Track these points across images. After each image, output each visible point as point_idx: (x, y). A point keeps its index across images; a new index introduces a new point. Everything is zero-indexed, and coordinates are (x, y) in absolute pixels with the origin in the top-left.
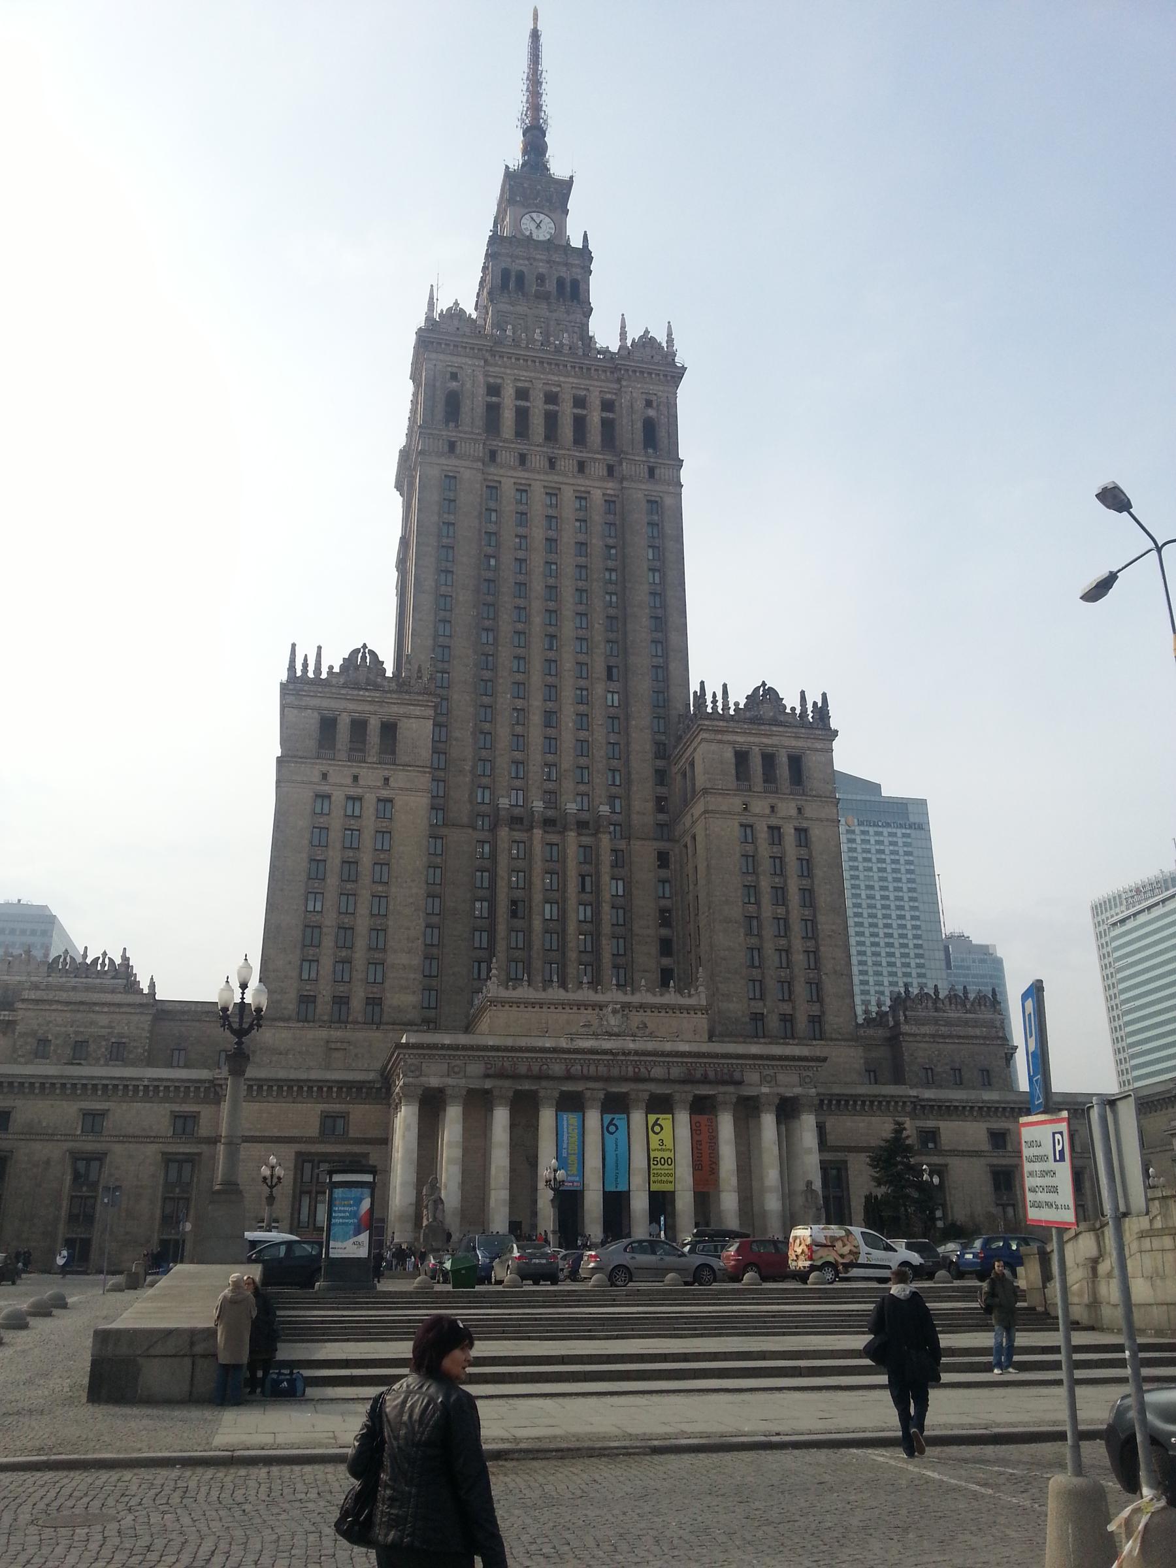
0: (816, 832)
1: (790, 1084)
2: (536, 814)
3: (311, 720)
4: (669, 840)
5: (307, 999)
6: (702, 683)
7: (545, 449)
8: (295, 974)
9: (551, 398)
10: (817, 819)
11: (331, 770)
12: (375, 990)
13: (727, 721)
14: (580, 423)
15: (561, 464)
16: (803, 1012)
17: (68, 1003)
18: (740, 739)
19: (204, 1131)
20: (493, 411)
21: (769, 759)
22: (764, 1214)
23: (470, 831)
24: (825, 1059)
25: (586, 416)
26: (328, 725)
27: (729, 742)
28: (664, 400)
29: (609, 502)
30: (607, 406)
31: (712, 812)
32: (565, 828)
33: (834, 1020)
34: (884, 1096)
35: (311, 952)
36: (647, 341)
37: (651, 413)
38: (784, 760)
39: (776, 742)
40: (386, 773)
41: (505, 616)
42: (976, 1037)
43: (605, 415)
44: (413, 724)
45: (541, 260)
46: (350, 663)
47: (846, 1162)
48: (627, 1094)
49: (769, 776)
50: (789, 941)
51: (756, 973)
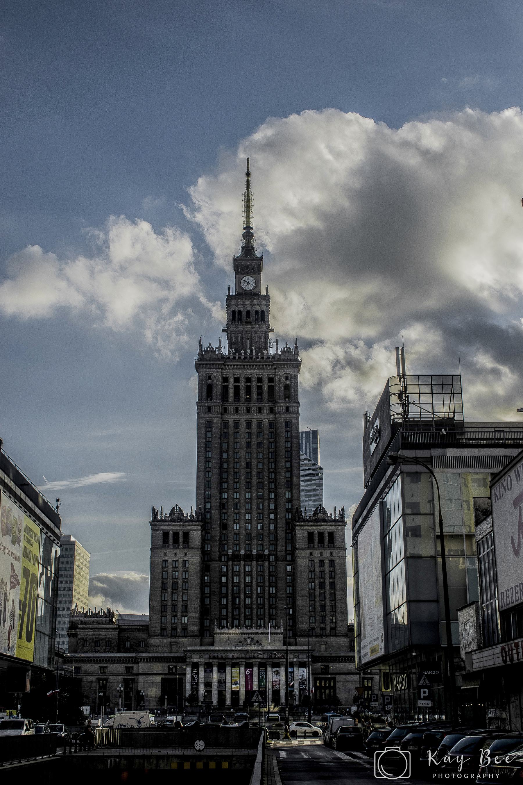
0: (337, 561)
3: (160, 534)
5: (163, 629)
8: (159, 621)
9: (248, 380)
11: (167, 551)
15: (253, 410)
17: (92, 629)
18: (310, 528)
19: (135, 672)
20: (225, 389)
25: (262, 386)
26: (166, 535)
27: (306, 530)
29: (270, 424)
30: (271, 380)
34: (350, 656)
37: (288, 382)
44: (194, 533)
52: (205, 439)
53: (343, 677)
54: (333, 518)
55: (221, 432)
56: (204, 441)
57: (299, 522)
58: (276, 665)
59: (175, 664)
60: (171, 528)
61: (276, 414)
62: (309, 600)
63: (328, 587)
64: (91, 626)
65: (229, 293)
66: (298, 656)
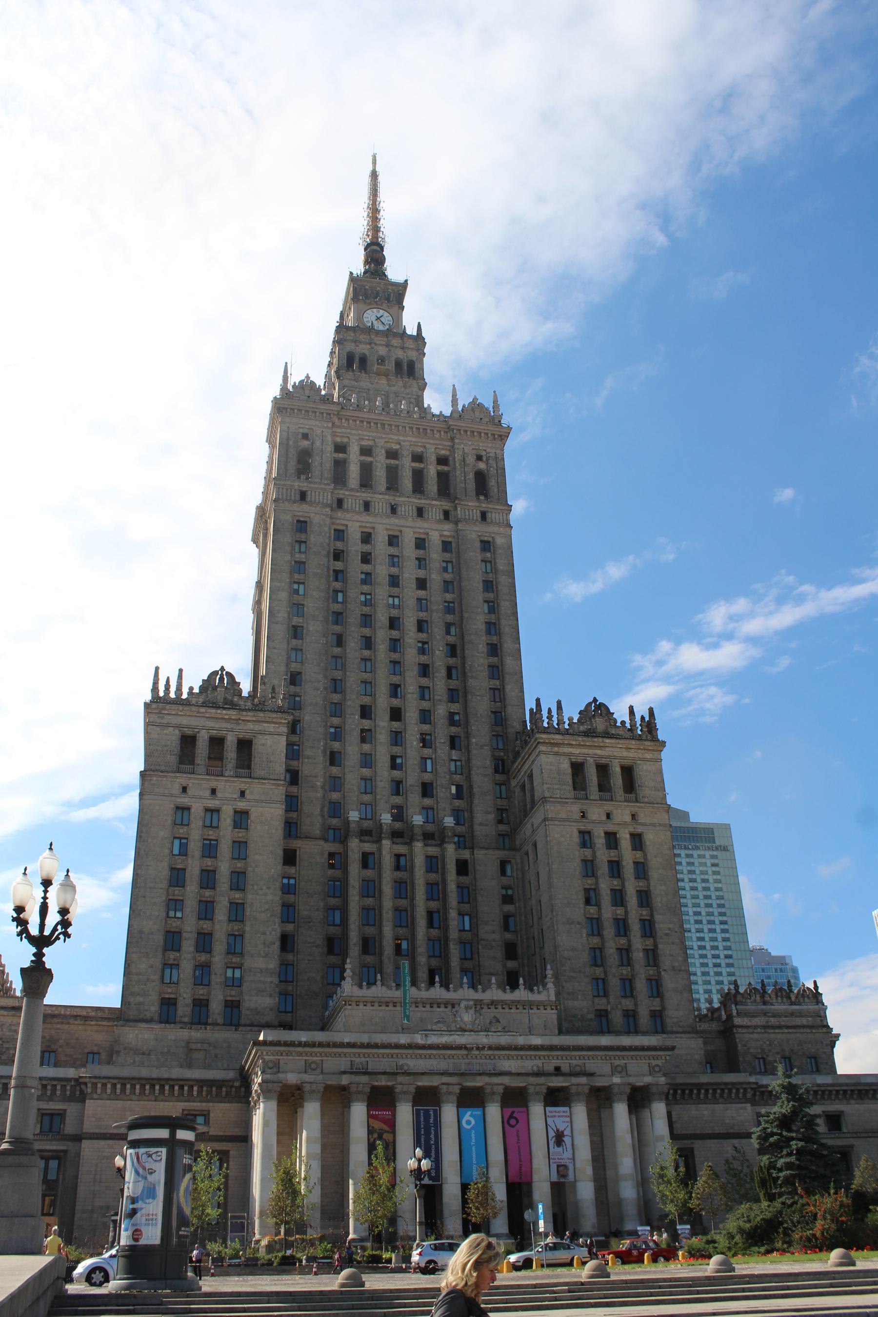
0: (650, 837)
1: (640, 1073)
2: (385, 827)
3: (172, 738)
4: (511, 849)
6: (538, 701)
7: (387, 497)
8: (156, 977)
9: (392, 454)
10: (651, 824)
11: (190, 783)
12: (233, 993)
13: (563, 734)
15: (401, 510)
16: (645, 1006)
21: (603, 769)
22: (620, 1202)
23: (322, 842)
24: (673, 1048)
26: (188, 741)
27: (564, 754)
28: (492, 455)
30: (442, 461)
31: (552, 819)
32: (412, 839)
33: (675, 1014)
34: (726, 1084)
35: (172, 957)
36: (475, 406)
37: (482, 466)
38: (618, 769)
39: (610, 753)
40: (243, 787)
41: (352, 644)
42: (803, 1027)
44: (268, 740)
45: (381, 345)
46: (208, 685)
48: (482, 1088)
49: (604, 787)
50: (629, 941)
51: (599, 971)
52: (292, 554)
53: (713, 1144)
55: (329, 545)
56: (288, 557)
58: (555, 1098)
59: (204, 1106)
63: (632, 900)
66: (625, 1068)
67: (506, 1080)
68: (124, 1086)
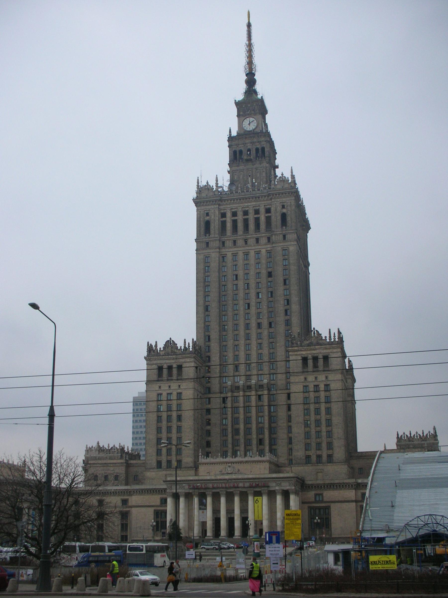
0: (333, 386)
1: (286, 486)
7: (243, 237)
8: (155, 454)
10: (333, 380)
14: (257, 221)
16: (325, 453)
17: (101, 464)
18: (304, 353)
26: (160, 369)
27: (299, 355)
28: (289, 204)
29: (269, 252)
30: (268, 211)
31: (292, 383)
37: (284, 211)
40: (179, 384)
43: (267, 215)
47: (330, 506)
49: (315, 366)
54: (328, 340)
57: (292, 347)
58: (258, 494)
60: (164, 362)
61: (273, 243)
62: (305, 427)
64: (100, 462)
65: (230, 135)
67: (241, 489)
68: (142, 491)
